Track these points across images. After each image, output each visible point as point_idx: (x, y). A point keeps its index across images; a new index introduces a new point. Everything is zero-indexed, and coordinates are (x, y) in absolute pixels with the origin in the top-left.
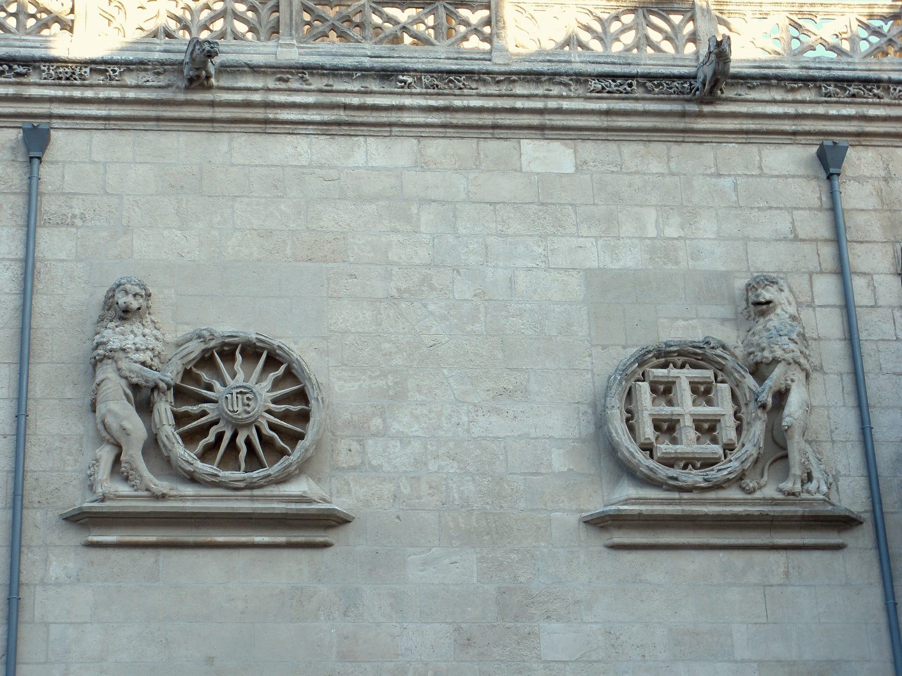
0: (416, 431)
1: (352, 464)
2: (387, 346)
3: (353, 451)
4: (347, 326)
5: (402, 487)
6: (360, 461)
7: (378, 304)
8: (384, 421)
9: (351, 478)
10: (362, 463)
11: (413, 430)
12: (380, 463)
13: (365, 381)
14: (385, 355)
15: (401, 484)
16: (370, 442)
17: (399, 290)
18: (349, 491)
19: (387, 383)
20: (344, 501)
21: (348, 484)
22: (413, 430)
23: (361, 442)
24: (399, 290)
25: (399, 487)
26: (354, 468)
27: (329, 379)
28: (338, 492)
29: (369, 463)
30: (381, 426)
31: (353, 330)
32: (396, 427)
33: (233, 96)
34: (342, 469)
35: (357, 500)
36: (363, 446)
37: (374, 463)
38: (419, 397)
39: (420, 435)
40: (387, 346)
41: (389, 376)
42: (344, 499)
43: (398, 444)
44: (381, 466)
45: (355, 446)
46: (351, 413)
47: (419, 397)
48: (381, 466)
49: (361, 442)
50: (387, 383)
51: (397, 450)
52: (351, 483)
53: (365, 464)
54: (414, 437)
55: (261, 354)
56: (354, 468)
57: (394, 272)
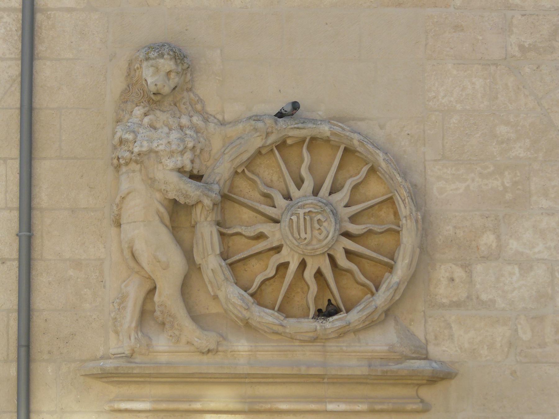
0: (539, 252)
1: (455, 299)
2: (502, 130)
3: (457, 280)
4: (451, 101)
5: (520, 331)
6: (466, 294)
7: (493, 68)
8: (498, 238)
9: (453, 318)
10: (468, 297)
11: (536, 250)
12: (491, 297)
13: (473, 180)
14: (502, 143)
15: (519, 326)
16: (479, 268)
17: (521, 47)
18: (451, 337)
19: (503, 184)
20: (444, 351)
21: (449, 326)
22: (536, 250)
23: (467, 267)
24: (521, 47)
25: (516, 331)
26: (457, 305)
27: (426, 179)
28: (436, 338)
29: (478, 298)
30: (494, 245)
31: (459, 107)
32: (514, 245)
33: (367, 312)
34: (442, 306)
35: (461, 348)
36: (470, 274)
37: (484, 297)
38: (545, 203)
39: (546, 257)
40: (502, 130)
41: (506, 173)
42: (444, 348)
43: (517, 270)
44: (493, 301)
45: (459, 273)
46: (455, 227)
47: (545, 203)
48: (493, 301)
49: (467, 267)
50: (503, 184)
51: (515, 278)
52: (453, 325)
53: (472, 299)
54: (538, 260)
55: (339, 147)
56: (457, 305)
57: (515, 22)
